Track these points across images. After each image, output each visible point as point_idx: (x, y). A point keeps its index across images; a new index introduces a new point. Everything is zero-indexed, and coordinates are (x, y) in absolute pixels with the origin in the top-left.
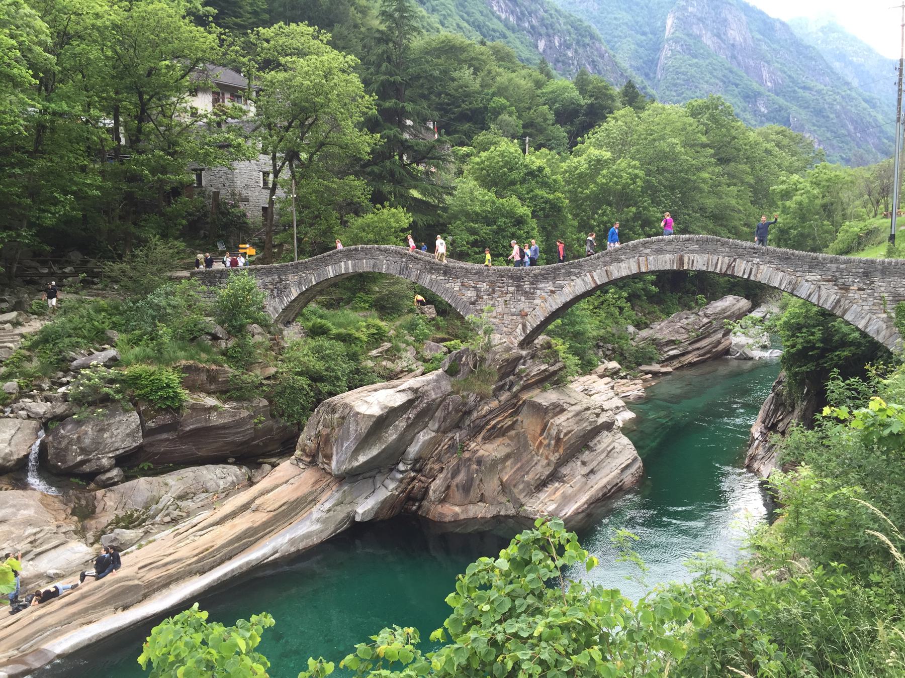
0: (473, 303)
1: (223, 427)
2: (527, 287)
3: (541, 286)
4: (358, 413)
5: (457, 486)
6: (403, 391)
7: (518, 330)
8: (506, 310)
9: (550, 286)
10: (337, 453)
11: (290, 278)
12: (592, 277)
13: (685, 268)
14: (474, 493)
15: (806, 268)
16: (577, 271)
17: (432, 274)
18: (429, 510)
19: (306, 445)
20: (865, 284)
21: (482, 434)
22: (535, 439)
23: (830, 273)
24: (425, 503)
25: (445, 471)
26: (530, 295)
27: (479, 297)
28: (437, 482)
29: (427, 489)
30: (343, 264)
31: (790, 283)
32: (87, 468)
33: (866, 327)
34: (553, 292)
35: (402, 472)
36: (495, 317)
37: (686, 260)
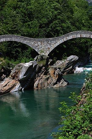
26: (50, 44)
35: (29, 81)
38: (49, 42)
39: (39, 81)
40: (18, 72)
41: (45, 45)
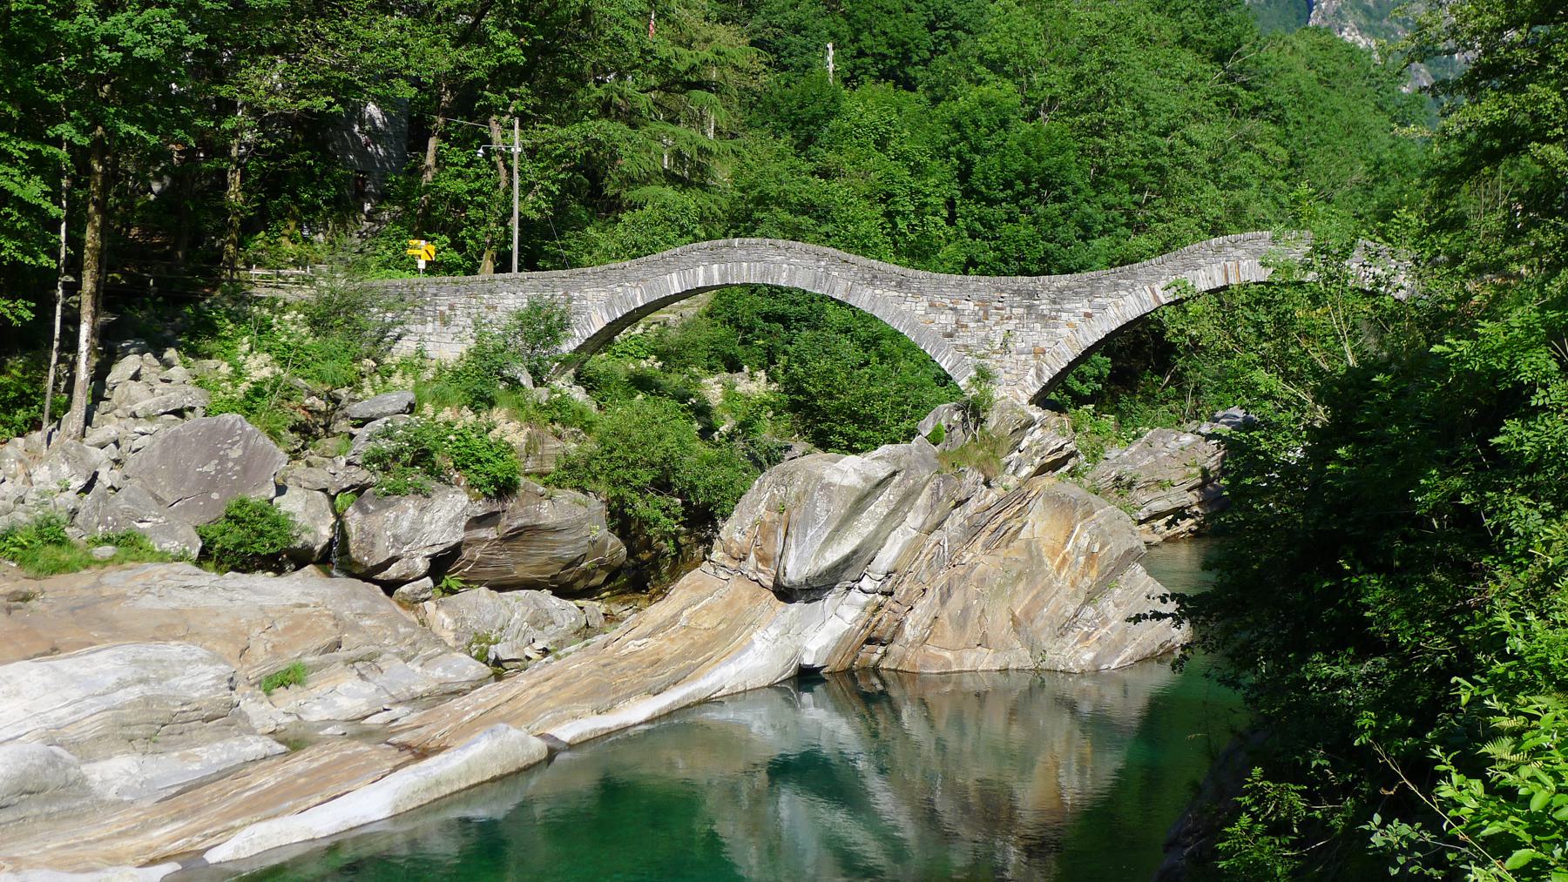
0: (950, 335)
1: (554, 530)
2: (1044, 306)
3: (1068, 306)
4: (830, 484)
5: (949, 615)
6: (881, 458)
7: (1028, 378)
9: (1083, 306)
10: (797, 547)
11: (590, 296)
12: (1153, 292)
14: (972, 632)
16: (1128, 282)
17: (876, 287)
18: (903, 657)
21: (982, 538)
22: (1055, 553)
24: (895, 648)
25: (929, 594)
27: (961, 325)
28: (918, 610)
29: (901, 623)
30: (701, 270)
32: (393, 572)
38: (1044, 306)
39: (946, 595)
41: (1011, 325)
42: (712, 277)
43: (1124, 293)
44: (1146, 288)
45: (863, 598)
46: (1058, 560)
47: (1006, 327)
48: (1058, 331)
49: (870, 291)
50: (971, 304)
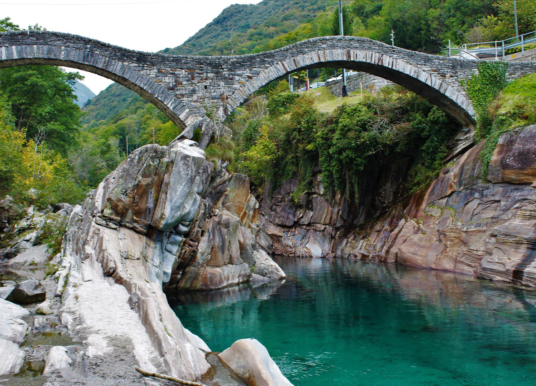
0: (172, 89)
2: (226, 73)
8: (207, 94)
9: (247, 73)
12: (283, 65)
13: (352, 59)
15: (423, 62)
17: (124, 61)
19: (120, 200)
20: (453, 73)
23: (435, 66)
26: (229, 81)
27: (178, 83)
29: (195, 252)
31: (415, 72)
33: (457, 100)
34: (250, 78)
36: (196, 101)
37: (352, 54)
40: (148, 185)
41: (207, 83)
42: (12, 54)
43: (268, 65)
44: (279, 63)
45: (180, 238)
46: (242, 213)
47: (204, 84)
48: (234, 86)
49: (120, 63)
50: (183, 71)
